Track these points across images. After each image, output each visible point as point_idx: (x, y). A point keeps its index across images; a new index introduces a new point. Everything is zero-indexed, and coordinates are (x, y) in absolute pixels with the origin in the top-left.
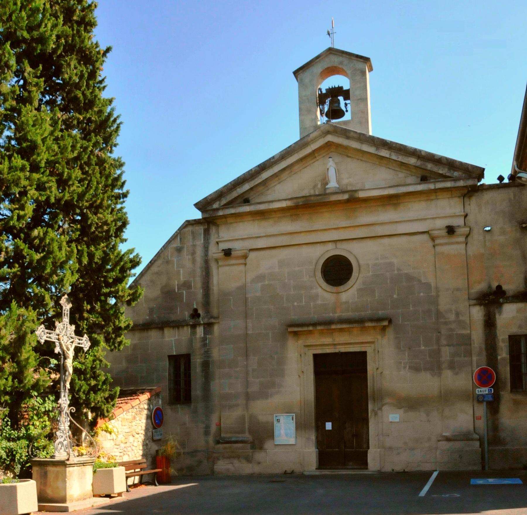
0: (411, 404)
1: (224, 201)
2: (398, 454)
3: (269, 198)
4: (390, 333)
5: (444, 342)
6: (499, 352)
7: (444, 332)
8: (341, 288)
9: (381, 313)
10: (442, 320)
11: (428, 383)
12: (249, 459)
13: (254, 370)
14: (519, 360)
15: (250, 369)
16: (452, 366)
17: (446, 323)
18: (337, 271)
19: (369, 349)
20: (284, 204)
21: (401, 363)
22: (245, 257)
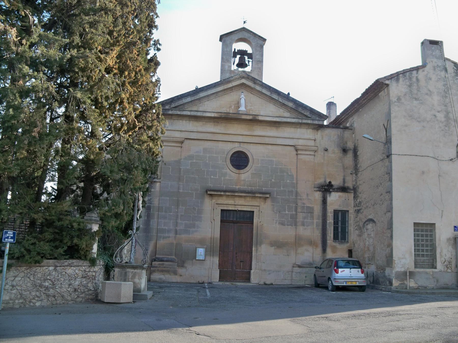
0: (278, 245)
1: (173, 105)
2: (269, 274)
3: (201, 109)
4: (269, 202)
5: (299, 210)
6: (328, 218)
7: (299, 204)
8: (242, 171)
9: (264, 189)
10: (299, 197)
11: (288, 233)
12: (175, 273)
13: (181, 215)
14: (338, 224)
15: (179, 214)
16: (303, 225)
17: (301, 199)
18: (240, 160)
19: (255, 210)
20: (213, 115)
21: (274, 220)
22: (182, 142)
